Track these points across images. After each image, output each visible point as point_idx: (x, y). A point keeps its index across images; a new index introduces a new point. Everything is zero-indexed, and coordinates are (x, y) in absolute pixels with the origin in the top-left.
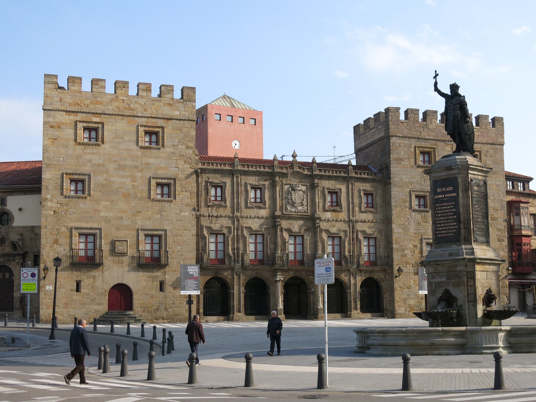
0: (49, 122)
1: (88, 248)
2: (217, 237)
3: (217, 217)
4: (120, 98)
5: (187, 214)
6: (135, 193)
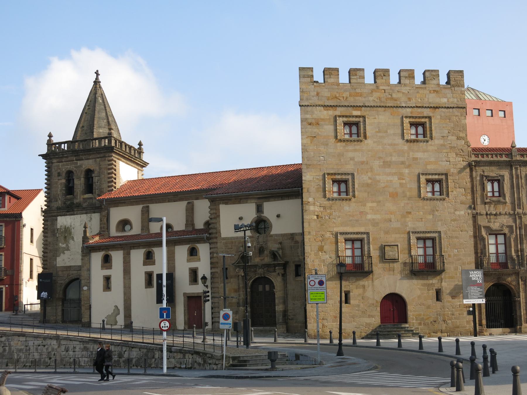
0: (306, 119)
1: (356, 255)
2: (496, 238)
3: (496, 215)
4: (381, 88)
5: (462, 213)
6: (404, 192)
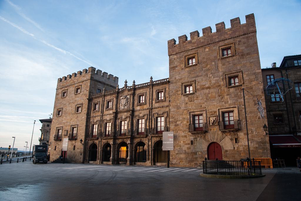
5: (84, 117)
